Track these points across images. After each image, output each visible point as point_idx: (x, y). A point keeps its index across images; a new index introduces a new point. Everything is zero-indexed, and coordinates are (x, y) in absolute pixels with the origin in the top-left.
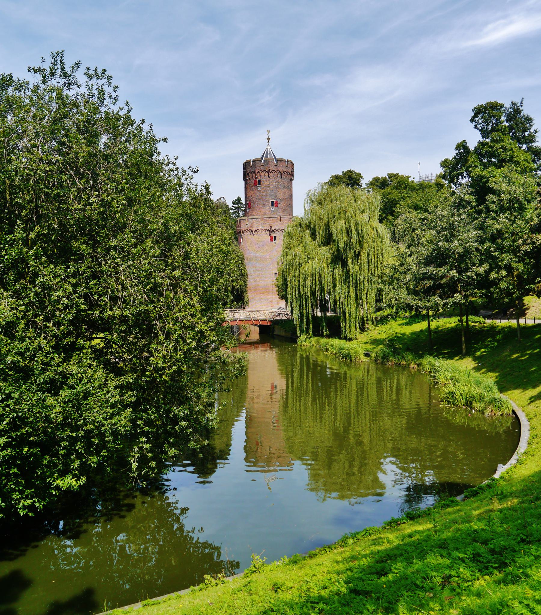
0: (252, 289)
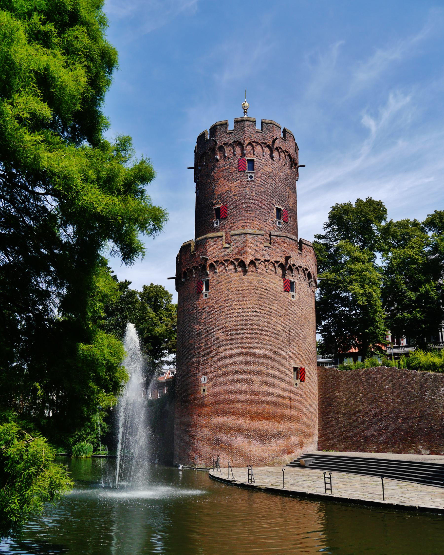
0: (239, 405)
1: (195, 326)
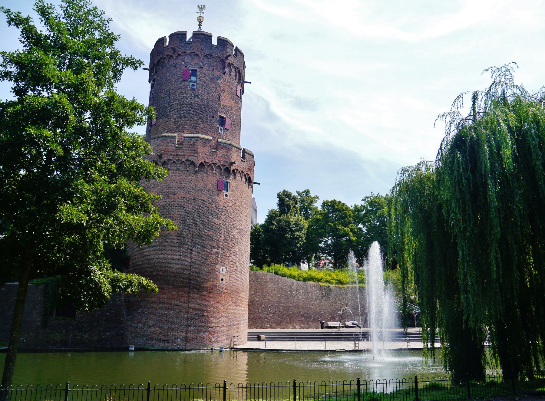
1: (214, 220)
